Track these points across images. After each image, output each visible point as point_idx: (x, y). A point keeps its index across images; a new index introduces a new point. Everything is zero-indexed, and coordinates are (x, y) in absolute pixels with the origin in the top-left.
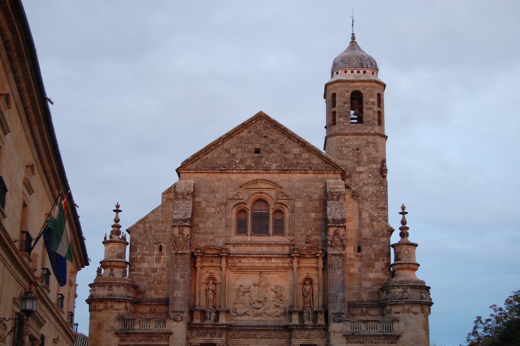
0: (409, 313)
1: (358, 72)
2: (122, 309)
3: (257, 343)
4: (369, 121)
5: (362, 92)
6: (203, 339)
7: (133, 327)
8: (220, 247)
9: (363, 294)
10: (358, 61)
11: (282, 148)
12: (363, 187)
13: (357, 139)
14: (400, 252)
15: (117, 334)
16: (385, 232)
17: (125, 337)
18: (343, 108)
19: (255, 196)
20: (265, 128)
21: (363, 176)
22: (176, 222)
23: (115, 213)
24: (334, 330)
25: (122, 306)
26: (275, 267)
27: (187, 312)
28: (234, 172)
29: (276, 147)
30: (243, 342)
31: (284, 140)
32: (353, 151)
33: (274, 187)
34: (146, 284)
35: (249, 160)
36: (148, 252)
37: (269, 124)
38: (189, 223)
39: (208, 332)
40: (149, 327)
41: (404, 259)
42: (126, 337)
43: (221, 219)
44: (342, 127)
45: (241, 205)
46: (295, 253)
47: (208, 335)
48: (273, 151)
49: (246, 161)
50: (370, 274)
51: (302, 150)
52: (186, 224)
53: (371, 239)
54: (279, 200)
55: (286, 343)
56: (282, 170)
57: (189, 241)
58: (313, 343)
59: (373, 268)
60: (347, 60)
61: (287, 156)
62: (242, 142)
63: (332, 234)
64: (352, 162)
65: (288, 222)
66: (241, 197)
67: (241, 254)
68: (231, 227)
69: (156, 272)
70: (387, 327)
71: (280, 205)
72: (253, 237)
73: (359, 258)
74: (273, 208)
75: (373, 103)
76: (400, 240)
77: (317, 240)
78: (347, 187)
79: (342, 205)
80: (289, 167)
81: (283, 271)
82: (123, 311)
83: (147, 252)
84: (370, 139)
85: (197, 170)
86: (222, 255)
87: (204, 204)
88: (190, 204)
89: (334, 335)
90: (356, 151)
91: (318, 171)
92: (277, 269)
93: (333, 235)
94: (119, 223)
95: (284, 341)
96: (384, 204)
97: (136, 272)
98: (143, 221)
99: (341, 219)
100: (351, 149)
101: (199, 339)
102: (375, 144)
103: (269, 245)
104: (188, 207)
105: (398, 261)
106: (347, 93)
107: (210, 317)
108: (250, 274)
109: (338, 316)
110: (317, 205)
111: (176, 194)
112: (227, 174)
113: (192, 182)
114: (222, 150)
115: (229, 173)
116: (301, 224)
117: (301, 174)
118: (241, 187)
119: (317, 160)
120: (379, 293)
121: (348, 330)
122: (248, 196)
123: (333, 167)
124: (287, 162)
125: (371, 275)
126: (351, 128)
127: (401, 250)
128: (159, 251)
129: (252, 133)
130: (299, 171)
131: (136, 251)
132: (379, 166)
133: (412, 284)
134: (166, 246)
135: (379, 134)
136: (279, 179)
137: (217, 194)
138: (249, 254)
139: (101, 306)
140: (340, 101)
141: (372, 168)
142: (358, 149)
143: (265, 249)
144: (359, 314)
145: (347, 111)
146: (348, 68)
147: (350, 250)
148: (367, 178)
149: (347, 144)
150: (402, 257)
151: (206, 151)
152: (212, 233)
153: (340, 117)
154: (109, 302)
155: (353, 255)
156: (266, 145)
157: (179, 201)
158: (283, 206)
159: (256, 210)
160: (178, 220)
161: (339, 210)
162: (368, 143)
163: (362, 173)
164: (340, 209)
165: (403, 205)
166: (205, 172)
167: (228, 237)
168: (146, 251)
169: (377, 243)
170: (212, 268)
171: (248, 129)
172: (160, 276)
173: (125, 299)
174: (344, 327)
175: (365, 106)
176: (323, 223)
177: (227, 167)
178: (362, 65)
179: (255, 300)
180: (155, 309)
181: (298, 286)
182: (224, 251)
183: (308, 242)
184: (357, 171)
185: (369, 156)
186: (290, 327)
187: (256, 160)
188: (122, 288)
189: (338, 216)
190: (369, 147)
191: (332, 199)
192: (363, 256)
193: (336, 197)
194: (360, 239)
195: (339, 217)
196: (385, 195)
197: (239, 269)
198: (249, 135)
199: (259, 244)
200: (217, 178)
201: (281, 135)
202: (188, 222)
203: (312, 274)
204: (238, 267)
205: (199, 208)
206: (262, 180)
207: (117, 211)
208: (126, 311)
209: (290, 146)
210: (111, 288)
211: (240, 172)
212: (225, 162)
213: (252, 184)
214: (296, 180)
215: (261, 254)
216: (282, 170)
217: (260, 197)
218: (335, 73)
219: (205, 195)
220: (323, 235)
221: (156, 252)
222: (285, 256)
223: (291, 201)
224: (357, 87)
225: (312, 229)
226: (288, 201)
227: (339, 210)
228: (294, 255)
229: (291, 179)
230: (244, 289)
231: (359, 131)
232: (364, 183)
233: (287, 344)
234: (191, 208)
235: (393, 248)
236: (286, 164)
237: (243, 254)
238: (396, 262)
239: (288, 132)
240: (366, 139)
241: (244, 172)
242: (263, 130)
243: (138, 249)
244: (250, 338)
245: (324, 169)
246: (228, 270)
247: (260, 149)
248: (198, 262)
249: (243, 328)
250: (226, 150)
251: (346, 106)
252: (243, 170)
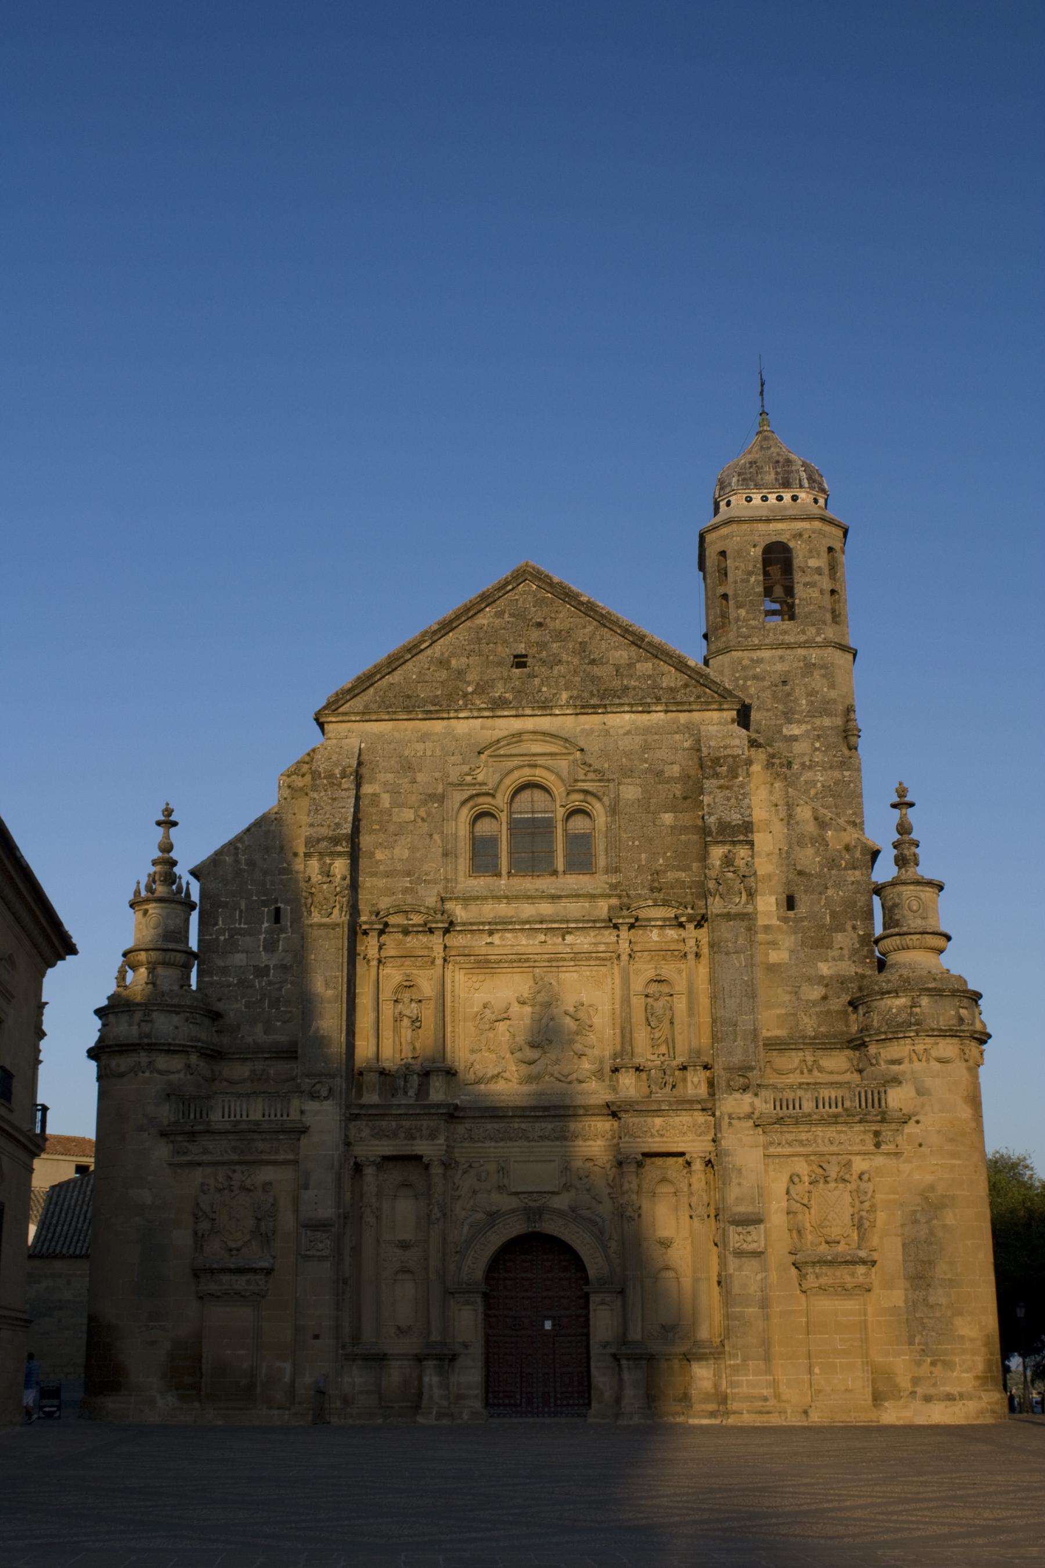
0: (928, 1060)
1: (780, 499)
2: (178, 1072)
4: (810, 613)
5: (791, 545)
6: (388, 1145)
7: (204, 1116)
8: (427, 908)
9: (804, 1017)
10: (777, 473)
11: (584, 651)
12: (801, 774)
13: (782, 658)
15: (163, 1134)
16: (858, 854)
17: (186, 1144)
18: (745, 584)
19: (516, 774)
20: (539, 602)
21: (800, 747)
22: (313, 846)
23: (160, 830)
24: (730, 1110)
25: (176, 1063)
26: (572, 955)
27: (344, 1074)
28: (461, 715)
29: (569, 648)
30: (492, 1150)
31: (587, 630)
32: (774, 688)
33: (565, 751)
34: (240, 1005)
35: (500, 685)
36: (246, 926)
37: (548, 592)
38: (347, 847)
40: (247, 1116)
41: (910, 922)
42: (188, 1141)
43: (431, 835)
44: (744, 630)
45: (481, 800)
46: (624, 917)
47: (402, 1135)
48: (560, 661)
49: (493, 687)
50: (819, 964)
51: (633, 654)
52: (339, 849)
53: (819, 876)
54: (580, 784)
56: (583, 707)
57: (346, 892)
59: (827, 948)
60: (750, 473)
61: (596, 671)
62: (479, 640)
63: (718, 863)
64: (770, 713)
65: (605, 839)
66: (480, 778)
67: (483, 923)
68: (455, 854)
69: (268, 975)
70: (870, 1101)
71: (581, 797)
72: (515, 881)
73: (791, 923)
74: (563, 804)
75: (818, 571)
76: (896, 875)
77: (681, 884)
78: (753, 744)
79: (743, 788)
80: (602, 699)
81: (593, 963)
82: (182, 1075)
83: (242, 926)
84: (814, 656)
85: (366, 715)
86: (434, 925)
87: (386, 800)
88: (349, 800)
90: (780, 687)
91: (675, 704)
92: (577, 957)
93: (721, 865)
94: (172, 854)
95: (599, 1146)
96: (853, 814)
97: (215, 978)
98: (232, 847)
99: (740, 822)
100: (767, 683)
101: (377, 1146)
102: (827, 668)
103: (554, 898)
104: (343, 808)
105: (894, 927)
106: (753, 550)
107: (405, 1086)
109: (739, 1075)
110: (678, 793)
111: (315, 774)
112: (446, 722)
113: (353, 743)
114: (431, 662)
115: (449, 718)
116: (637, 843)
117: (633, 715)
118: (479, 753)
119: (673, 678)
120: (845, 1013)
121: (767, 1111)
122: (497, 777)
123: (716, 695)
124: (597, 685)
125: (825, 969)
126: (766, 633)
127: (899, 898)
128: (273, 919)
129: (506, 615)
130: (627, 708)
131: (216, 924)
132: (839, 721)
133: (932, 985)
134: (291, 909)
135: (836, 643)
136: (578, 729)
137: (419, 774)
138: (505, 923)
139: (123, 1063)
140: (737, 568)
141: (822, 728)
142: (784, 682)
143: (546, 908)
144: (796, 1069)
145: (755, 592)
146: (755, 491)
147: (767, 905)
148: (810, 751)
149: (758, 670)
150: (904, 917)
151: (389, 663)
152: (409, 874)
153: (739, 606)
154: (143, 1054)
155: (776, 918)
156: (542, 646)
157: (323, 793)
158: (590, 798)
159: (520, 813)
160: (319, 841)
161: (733, 801)
162: (809, 668)
163: (796, 740)
164: (737, 799)
165: (901, 784)
166: (387, 717)
167: (447, 880)
168: (240, 924)
169: (837, 886)
170: (408, 962)
171: (494, 605)
172: (277, 986)
173: (184, 1046)
174: (757, 1102)
175: (798, 577)
176: (695, 837)
177: (444, 703)
178: (786, 484)
179: (522, 1042)
180: (264, 1070)
181: (634, 1000)
182: (439, 917)
183: (656, 888)
184: (786, 736)
185: (813, 698)
186: (614, 1108)
187: (517, 683)
188: (176, 1019)
189: (734, 817)
190: (812, 676)
191: (716, 775)
192: (802, 919)
193: (725, 768)
194: (791, 876)
195: (735, 818)
196: (854, 792)
197: (480, 961)
198: (497, 621)
199: (530, 898)
200: (420, 733)
201: (578, 620)
202: (344, 844)
203: (668, 970)
205: (373, 810)
206: (534, 732)
207: (168, 823)
208: (189, 1077)
209: (604, 645)
210: (147, 1018)
211: (476, 714)
212: (439, 693)
213: (508, 744)
214: (621, 731)
215: (536, 922)
216: (583, 707)
217: (530, 778)
218: (723, 504)
219: (390, 777)
220: (694, 870)
221: (266, 925)
223: (611, 785)
224: (779, 533)
225: (665, 853)
226: (602, 784)
227: (733, 801)
228: (620, 921)
229: (606, 727)
230: (493, 1013)
231: (788, 639)
232: (803, 765)
234: (352, 810)
235: (878, 898)
236: (595, 692)
237: (489, 923)
238: (888, 932)
239: (598, 609)
240: (805, 657)
241: (486, 714)
242: (534, 607)
243: (220, 919)
244: (511, 1139)
245: (692, 699)
246: (450, 966)
247: (526, 656)
248: (372, 946)
249: (491, 1114)
250: (441, 663)
251: (753, 579)
252: (485, 709)
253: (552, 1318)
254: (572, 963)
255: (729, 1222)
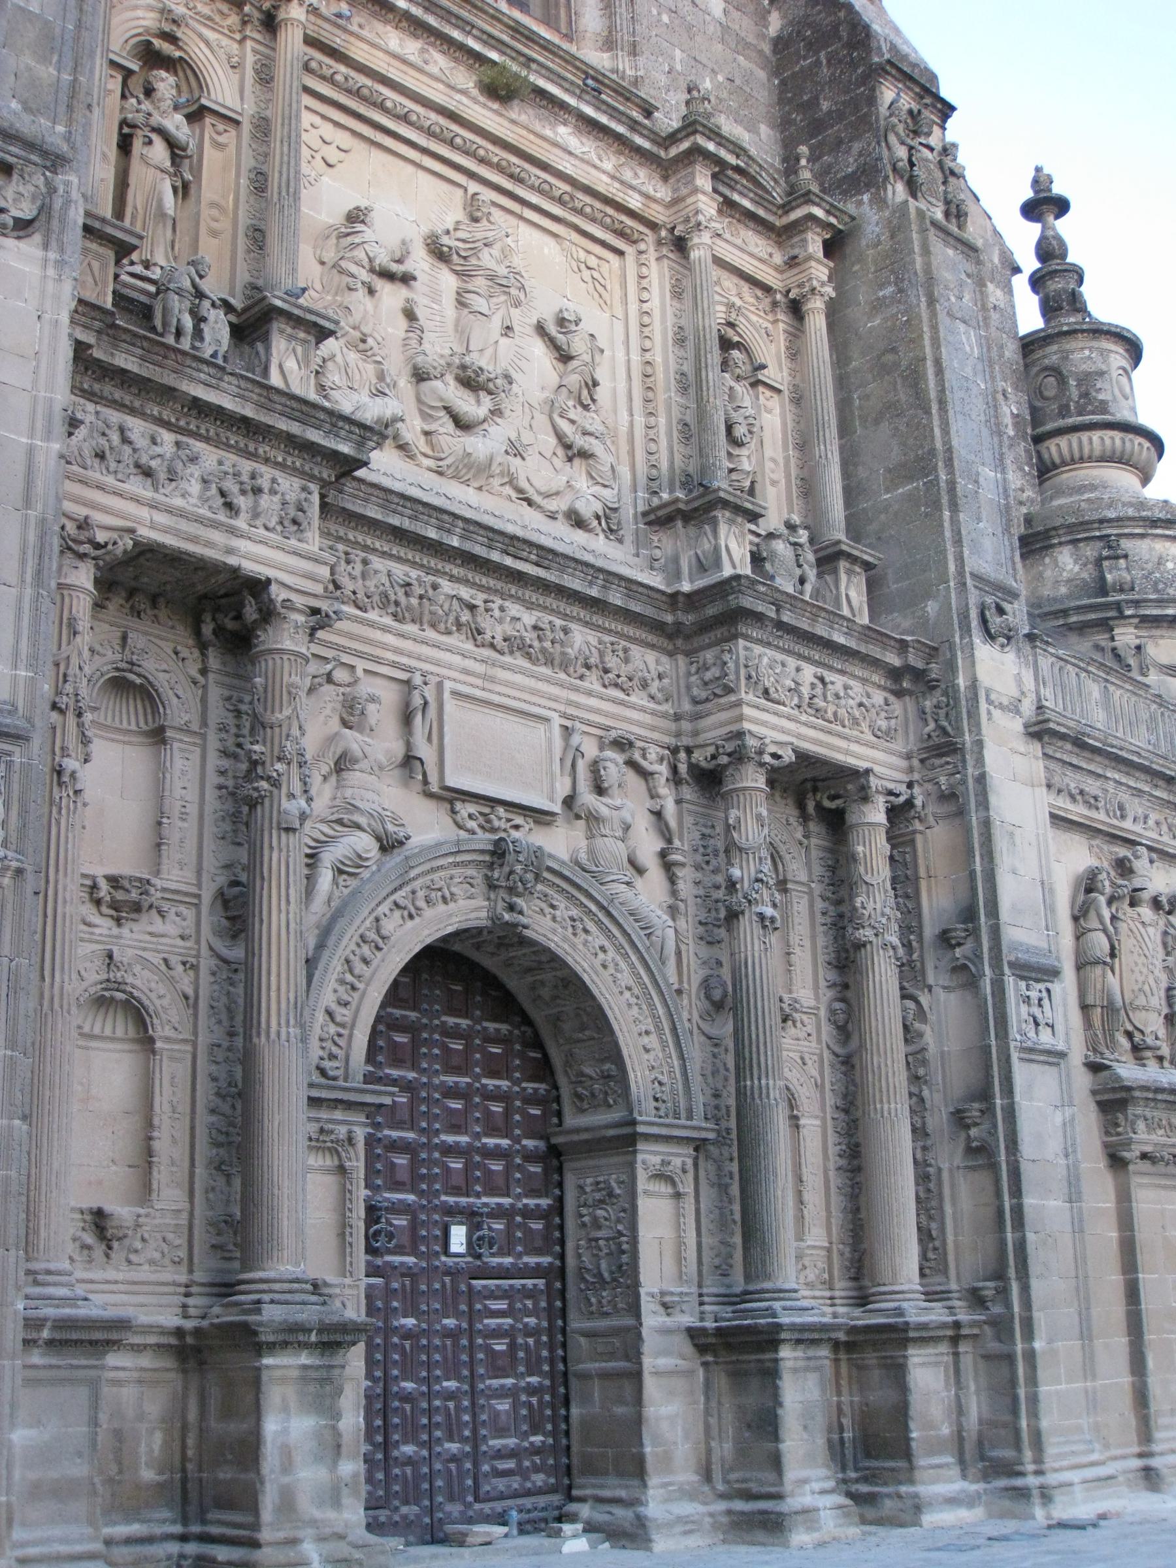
3: (485, 677)
14: (1101, 374)
39: (193, 459)
47: (195, 488)
55: (653, 728)
58: (847, 752)
89: (989, 713)
108: (410, 169)
197: (357, 93)
204: (353, 73)
222: (639, 141)
233: (656, 736)
249: (406, 524)
253: (472, 1218)
254: (556, 210)
255: (1012, 965)
